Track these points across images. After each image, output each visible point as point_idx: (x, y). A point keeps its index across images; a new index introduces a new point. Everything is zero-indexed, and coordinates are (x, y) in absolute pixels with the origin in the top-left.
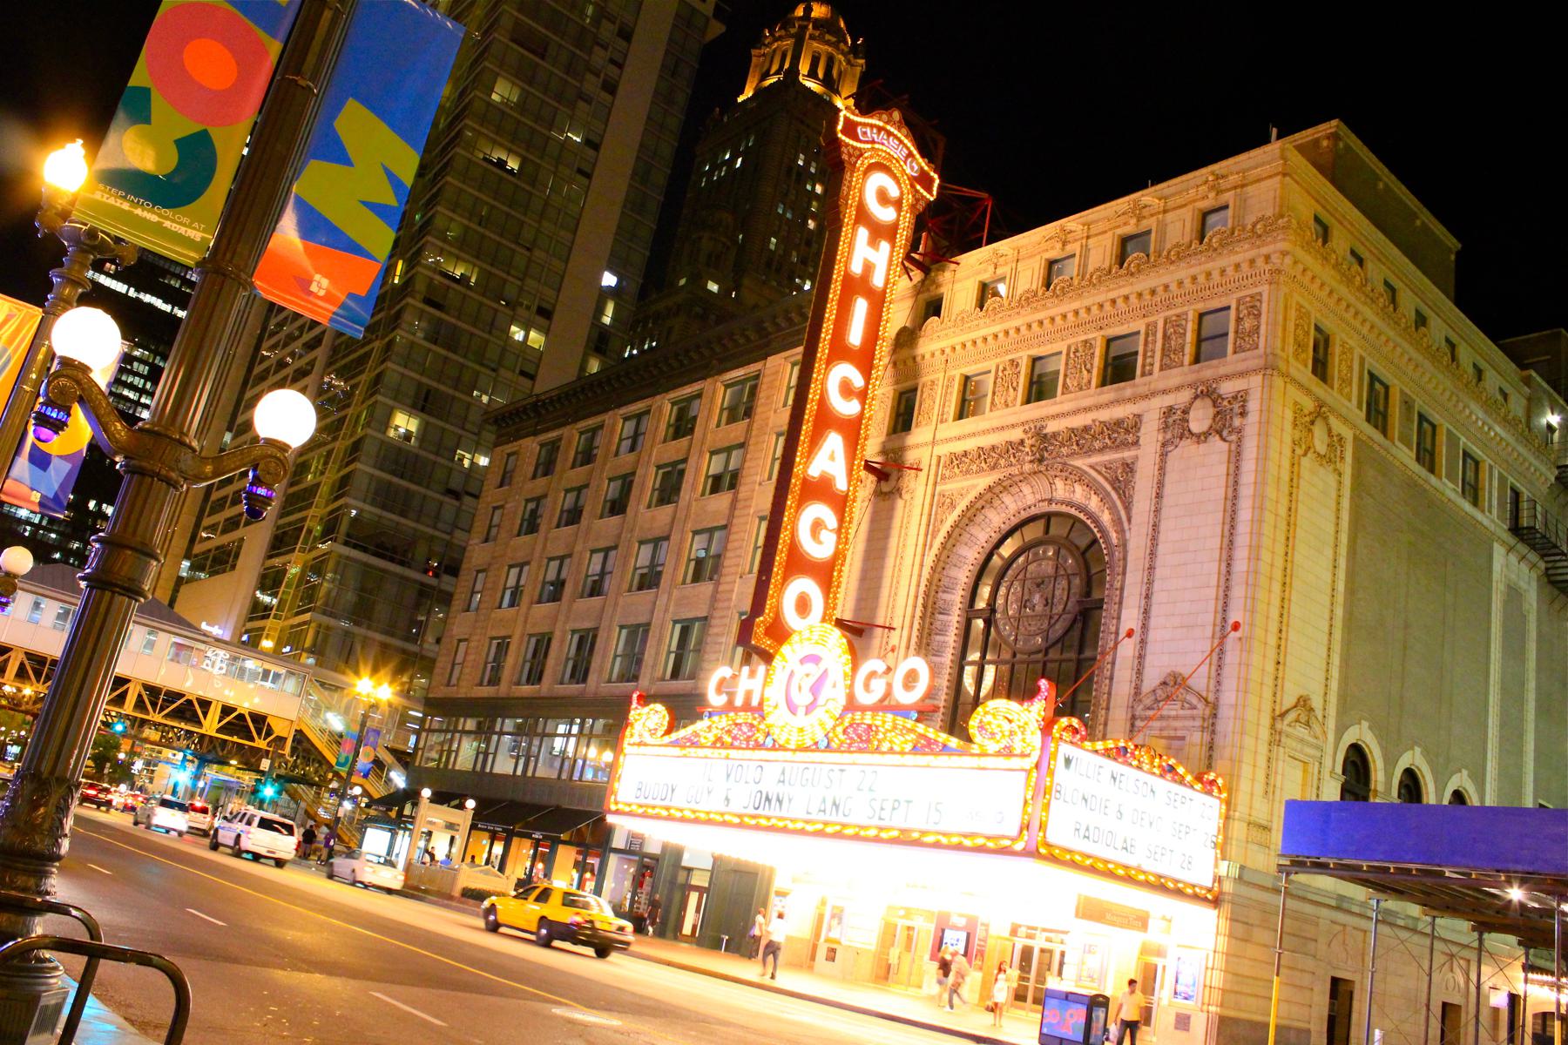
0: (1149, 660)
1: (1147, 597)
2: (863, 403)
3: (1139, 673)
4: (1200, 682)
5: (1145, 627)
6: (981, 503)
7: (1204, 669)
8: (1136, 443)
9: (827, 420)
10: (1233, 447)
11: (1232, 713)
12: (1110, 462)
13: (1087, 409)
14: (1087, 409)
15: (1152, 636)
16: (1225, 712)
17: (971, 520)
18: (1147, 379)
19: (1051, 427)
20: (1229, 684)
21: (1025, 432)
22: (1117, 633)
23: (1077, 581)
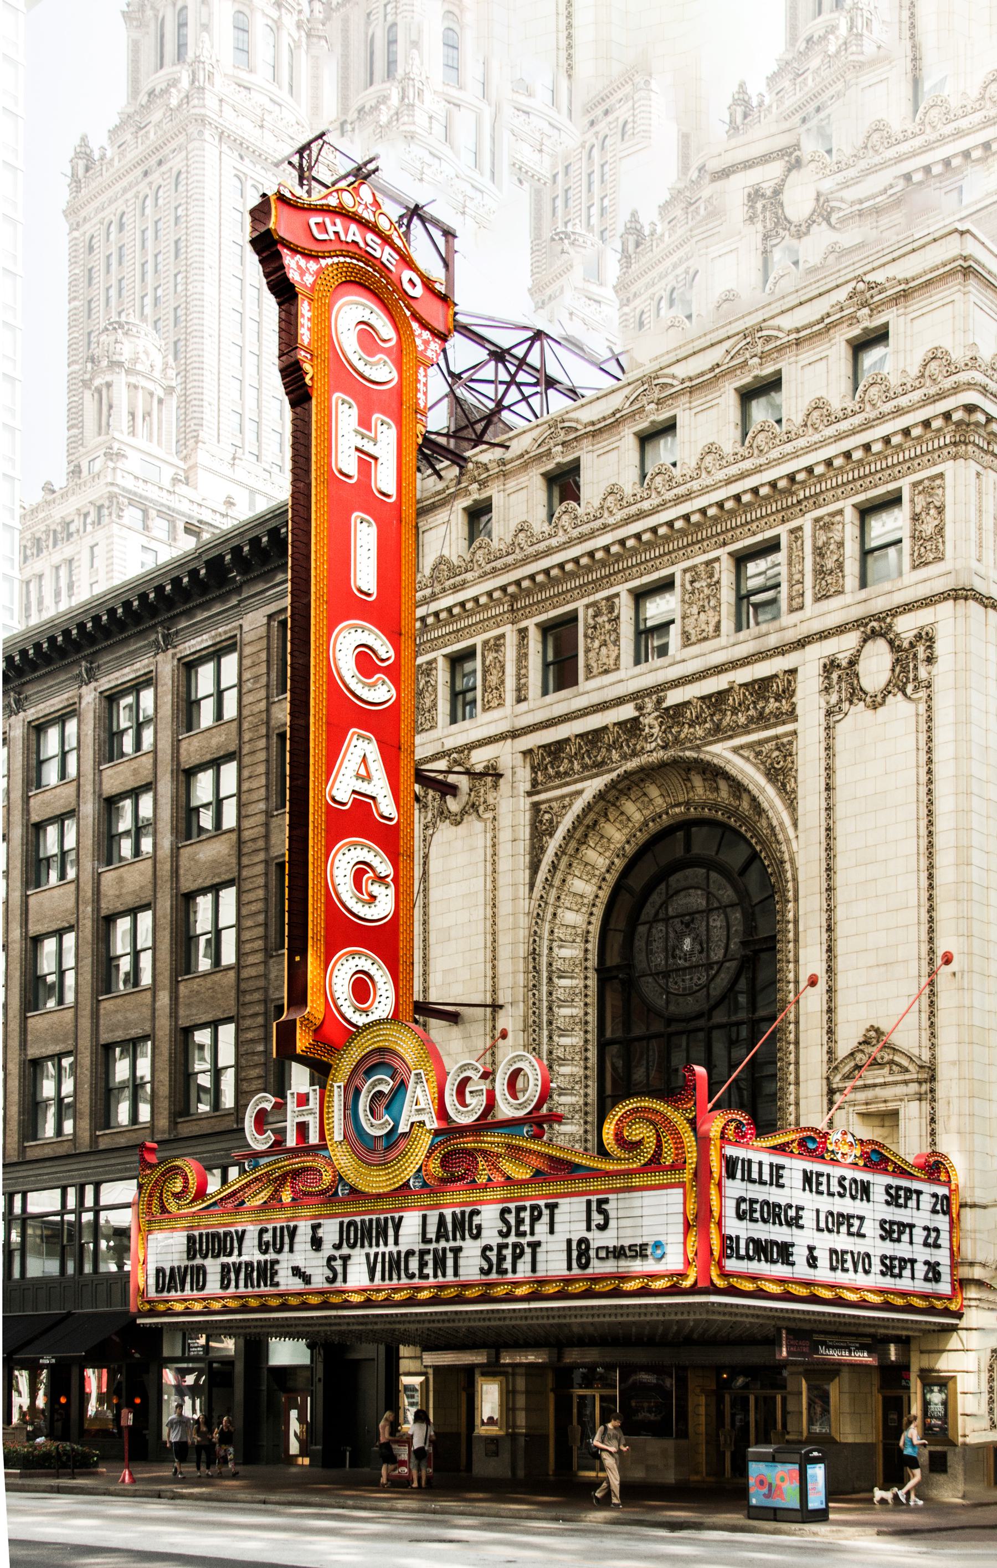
0: (842, 1015)
1: (829, 929)
2: (397, 683)
3: (830, 1031)
4: (908, 1038)
5: (830, 970)
6: (592, 816)
7: (912, 1018)
8: (792, 715)
9: (347, 714)
10: (922, 707)
11: (954, 1073)
12: (761, 743)
13: (719, 669)
14: (719, 669)
15: (842, 981)
16: (944, 1072)
17: (583, 841)
18: (798, 616)
19: (674, 697)
20: (946, 1035)
21: (640, 708)
22: (797, 982)
23: (737, 915)
